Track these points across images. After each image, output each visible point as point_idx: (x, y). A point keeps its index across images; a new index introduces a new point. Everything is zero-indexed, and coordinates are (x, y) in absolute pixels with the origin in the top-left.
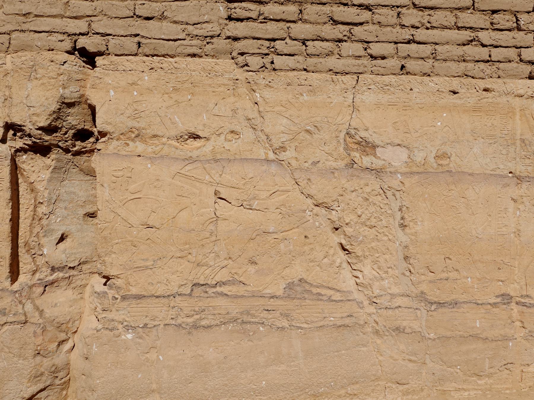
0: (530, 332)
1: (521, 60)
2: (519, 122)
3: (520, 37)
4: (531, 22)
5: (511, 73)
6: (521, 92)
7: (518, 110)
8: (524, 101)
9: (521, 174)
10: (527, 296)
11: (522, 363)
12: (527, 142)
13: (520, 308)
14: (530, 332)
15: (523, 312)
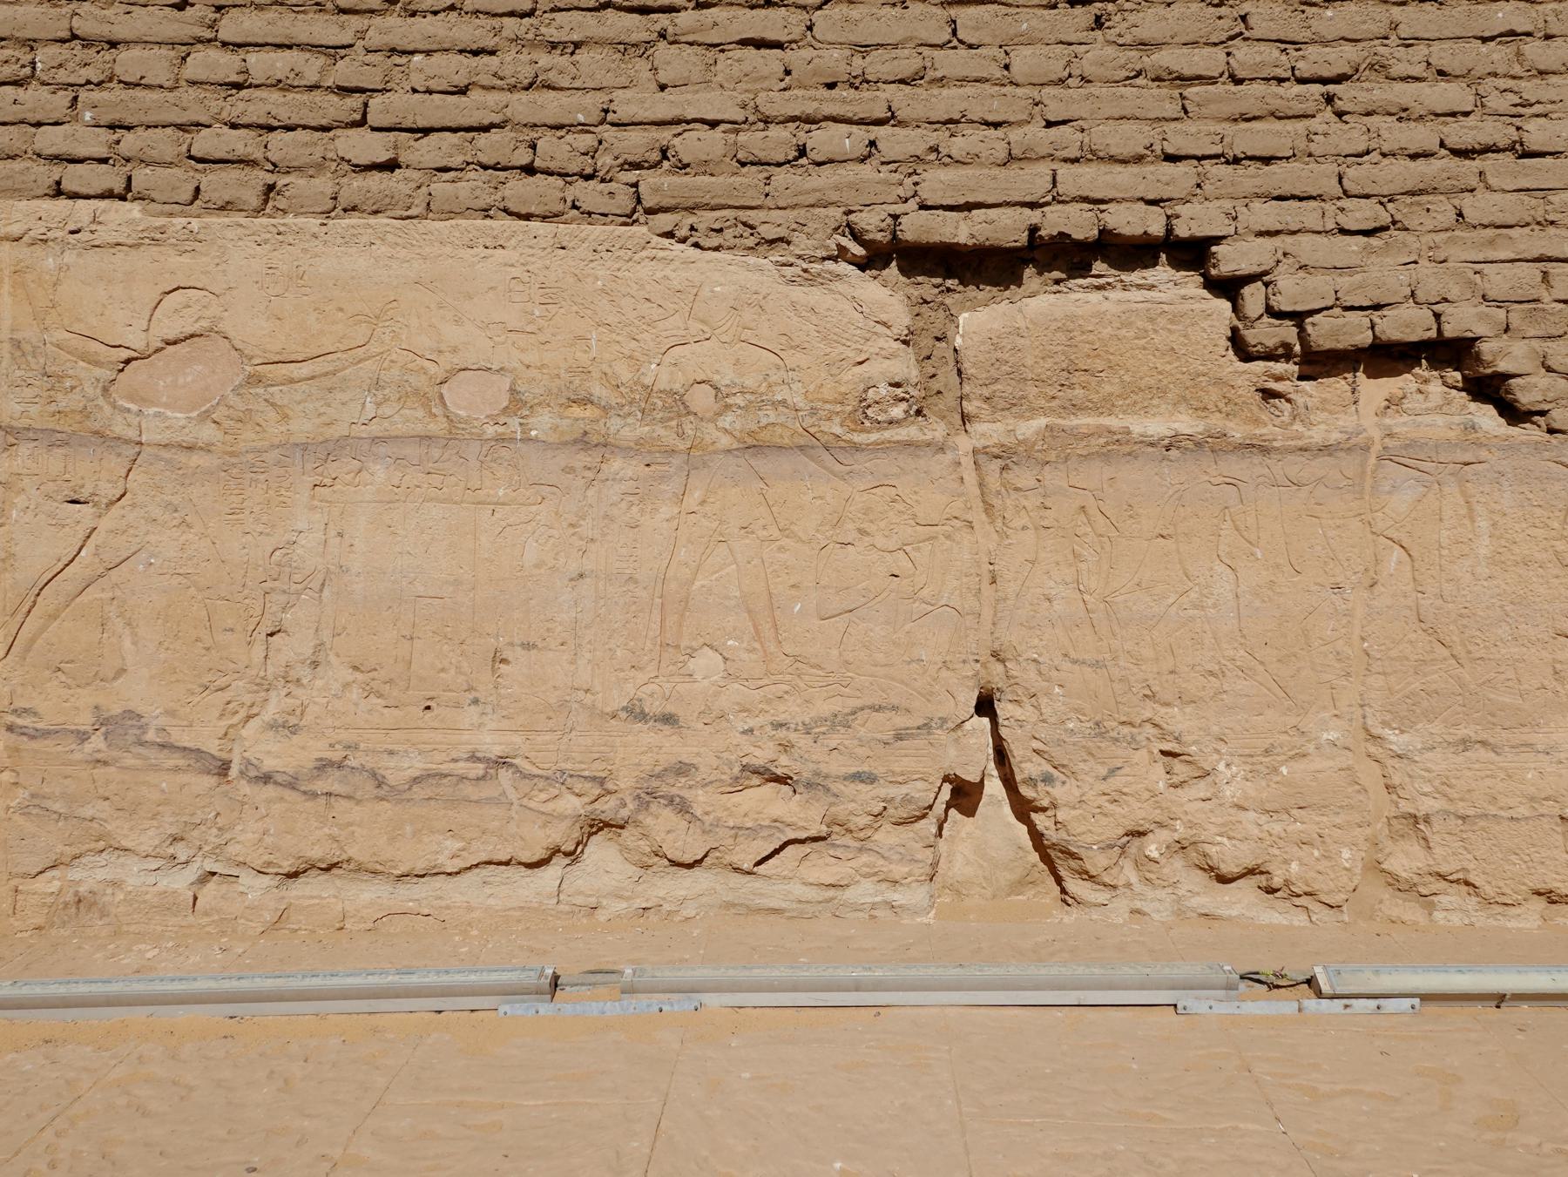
0: (33, 796)
1: (39, 155)
2: (8, 300)
3: (35, 99)
4: (60, 66)
5: (9, 183)
6: (16, 229)
7: (7, 272)
8: (21, 251)
9: (14, 423)
10: (25, 710)
11: (14, 871)
12: (27, 348)
13: (13, 736)
14: (33, 796)
15: (17, 750)
